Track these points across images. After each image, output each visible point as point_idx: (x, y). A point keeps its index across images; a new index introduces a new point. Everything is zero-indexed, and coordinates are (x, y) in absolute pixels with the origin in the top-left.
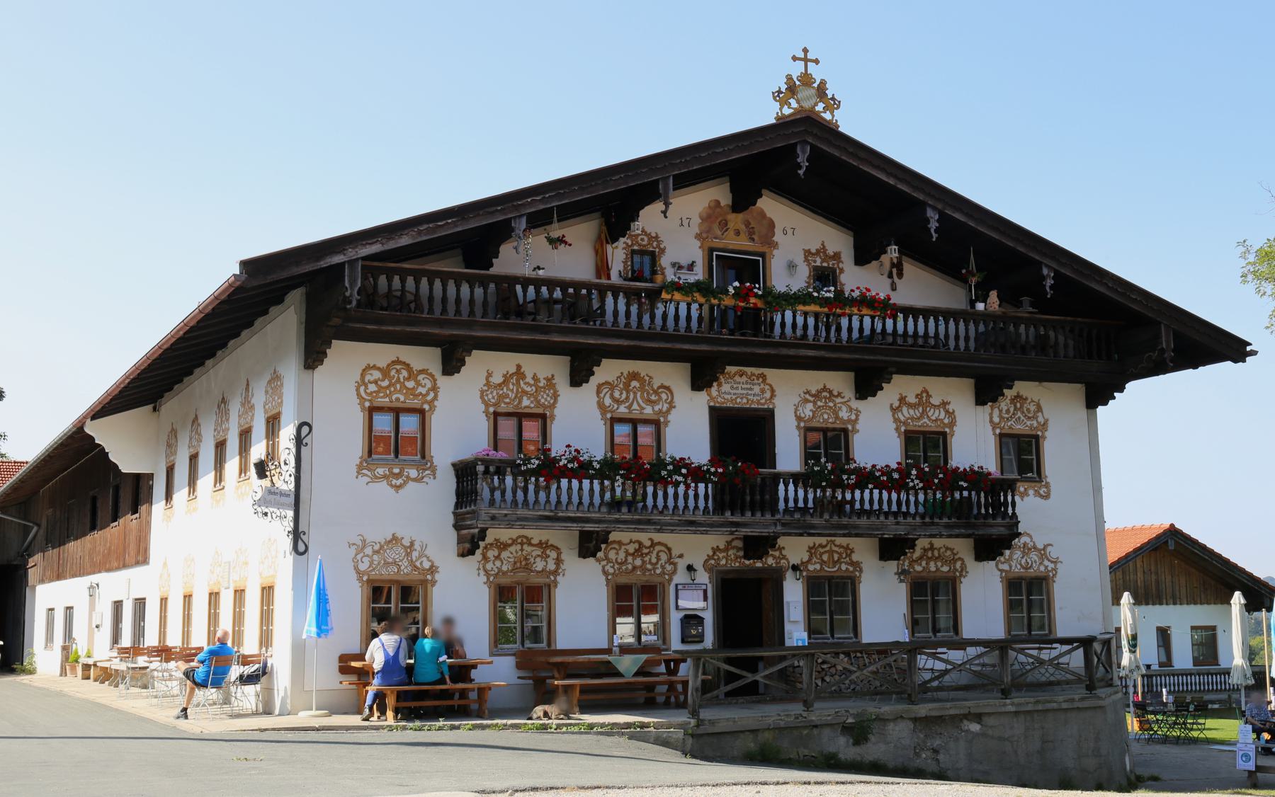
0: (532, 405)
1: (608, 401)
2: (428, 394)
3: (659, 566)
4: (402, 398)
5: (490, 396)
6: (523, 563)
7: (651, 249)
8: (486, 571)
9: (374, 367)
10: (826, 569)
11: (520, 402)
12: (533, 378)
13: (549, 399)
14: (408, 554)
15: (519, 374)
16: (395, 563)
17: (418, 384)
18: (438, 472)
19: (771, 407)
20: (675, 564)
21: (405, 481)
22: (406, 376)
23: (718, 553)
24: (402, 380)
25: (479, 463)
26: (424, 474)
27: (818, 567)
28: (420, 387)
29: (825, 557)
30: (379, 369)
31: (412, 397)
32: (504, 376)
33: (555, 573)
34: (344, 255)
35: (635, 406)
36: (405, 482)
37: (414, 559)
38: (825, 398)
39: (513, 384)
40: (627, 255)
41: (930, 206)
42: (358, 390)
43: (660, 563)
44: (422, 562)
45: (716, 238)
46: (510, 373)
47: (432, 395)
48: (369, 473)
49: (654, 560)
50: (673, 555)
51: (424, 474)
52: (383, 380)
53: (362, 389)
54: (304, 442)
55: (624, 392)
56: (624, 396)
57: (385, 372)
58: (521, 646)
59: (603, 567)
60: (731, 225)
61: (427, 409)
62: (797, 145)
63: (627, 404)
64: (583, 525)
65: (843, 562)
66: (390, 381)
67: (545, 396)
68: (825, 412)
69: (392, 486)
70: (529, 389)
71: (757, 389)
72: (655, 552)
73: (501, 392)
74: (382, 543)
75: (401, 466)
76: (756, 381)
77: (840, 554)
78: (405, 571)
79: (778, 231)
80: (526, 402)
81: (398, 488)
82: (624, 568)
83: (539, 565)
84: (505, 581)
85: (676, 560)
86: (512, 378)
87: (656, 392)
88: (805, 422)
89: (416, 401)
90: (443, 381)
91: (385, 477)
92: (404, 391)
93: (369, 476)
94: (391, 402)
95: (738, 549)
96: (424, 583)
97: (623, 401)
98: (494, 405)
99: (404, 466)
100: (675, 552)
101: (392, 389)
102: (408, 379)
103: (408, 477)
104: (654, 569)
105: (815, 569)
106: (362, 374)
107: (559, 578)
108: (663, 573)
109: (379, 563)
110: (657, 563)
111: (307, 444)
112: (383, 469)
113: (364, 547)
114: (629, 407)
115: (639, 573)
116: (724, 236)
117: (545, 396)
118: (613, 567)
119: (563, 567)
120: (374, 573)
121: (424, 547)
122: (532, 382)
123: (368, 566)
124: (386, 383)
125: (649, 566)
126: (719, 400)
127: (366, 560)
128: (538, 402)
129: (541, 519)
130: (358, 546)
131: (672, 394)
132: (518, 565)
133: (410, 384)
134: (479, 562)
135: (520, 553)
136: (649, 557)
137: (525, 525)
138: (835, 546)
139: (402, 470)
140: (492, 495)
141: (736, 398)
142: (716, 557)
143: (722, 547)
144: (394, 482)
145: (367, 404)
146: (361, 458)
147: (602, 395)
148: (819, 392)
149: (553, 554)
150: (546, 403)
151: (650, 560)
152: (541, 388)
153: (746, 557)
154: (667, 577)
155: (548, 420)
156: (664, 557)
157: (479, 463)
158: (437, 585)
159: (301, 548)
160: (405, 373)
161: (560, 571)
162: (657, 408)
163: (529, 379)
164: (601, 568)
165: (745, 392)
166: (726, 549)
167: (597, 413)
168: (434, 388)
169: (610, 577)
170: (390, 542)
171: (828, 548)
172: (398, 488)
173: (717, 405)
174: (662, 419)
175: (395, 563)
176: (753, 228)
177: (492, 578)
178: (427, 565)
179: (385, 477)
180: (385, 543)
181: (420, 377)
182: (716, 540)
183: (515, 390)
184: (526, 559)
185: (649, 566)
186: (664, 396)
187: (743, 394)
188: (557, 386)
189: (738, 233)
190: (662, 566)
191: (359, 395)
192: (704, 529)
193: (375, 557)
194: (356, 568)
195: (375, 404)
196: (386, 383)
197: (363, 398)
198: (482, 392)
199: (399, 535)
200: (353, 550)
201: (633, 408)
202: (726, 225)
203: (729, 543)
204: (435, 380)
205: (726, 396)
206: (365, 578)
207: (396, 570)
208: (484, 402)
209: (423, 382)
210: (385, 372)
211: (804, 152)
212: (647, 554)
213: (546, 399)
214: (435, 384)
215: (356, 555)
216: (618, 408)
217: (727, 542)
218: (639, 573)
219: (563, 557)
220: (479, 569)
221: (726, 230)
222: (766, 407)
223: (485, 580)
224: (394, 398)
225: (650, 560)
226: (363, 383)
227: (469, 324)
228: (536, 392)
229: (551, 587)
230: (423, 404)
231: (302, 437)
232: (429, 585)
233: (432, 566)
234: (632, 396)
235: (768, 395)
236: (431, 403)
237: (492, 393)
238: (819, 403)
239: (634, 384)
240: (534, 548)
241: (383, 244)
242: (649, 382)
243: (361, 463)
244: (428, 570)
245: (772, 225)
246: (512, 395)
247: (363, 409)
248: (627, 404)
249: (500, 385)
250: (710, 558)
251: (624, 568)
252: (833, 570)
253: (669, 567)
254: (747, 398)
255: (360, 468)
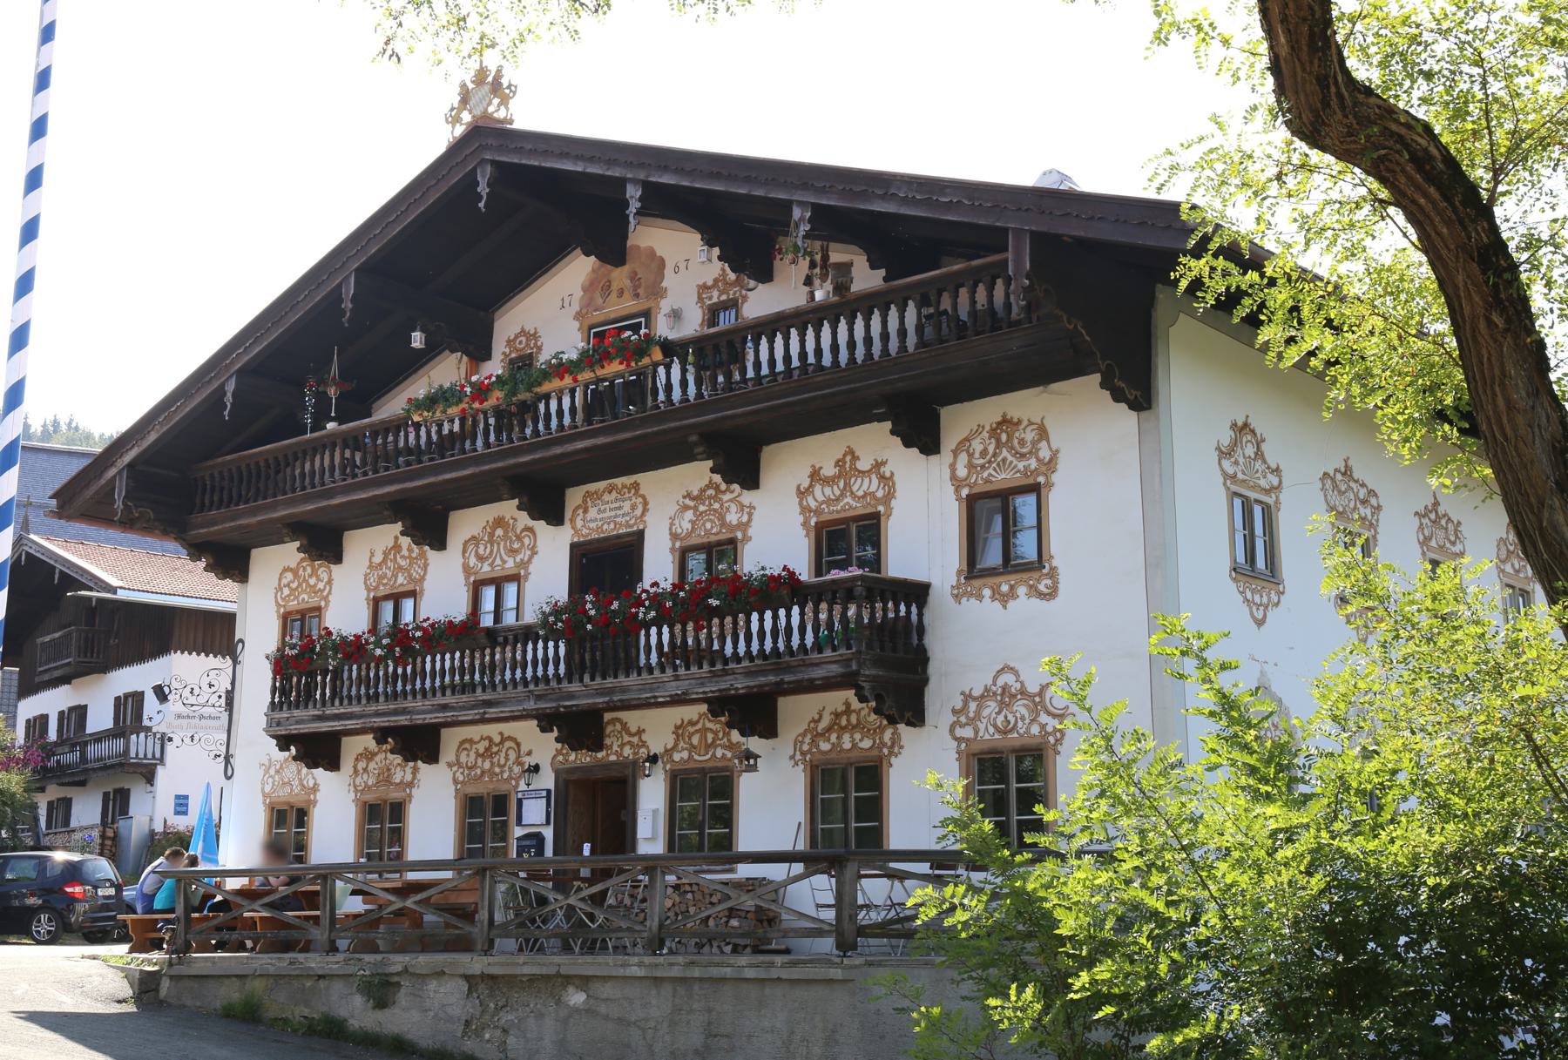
1: (473, 561)
4: (306, 597)
8: (355, 786)
17: (319, 579)
32: (384, 553)
33: (411, 785)
35: (498, 562)
38: (710, 497)
49: (502, 761)
56: (488, 550)
71: (627, 506)
80: (401, 580)
87: (519, 538)
88: (681, 539)
98: (376, 588)
100: (524, 749)
104: (502, 772)
108: (510, 778)
114: (491, 565)
119: (418, 776)
125: (497, 770)
127: (270, 780)
133: (312, 581)
148: (703, 491)
156: (512, 755)
159: (229, 773)
165: (613, 514)
174: (522, 572)
184: (389, 770)
185: (497, 770)
186: (526, 541)
194: (263, 790)
198: (366, 575)
200: (262, 772)
205: (592, 525)
212: (496, 753)
226: (280, 589)
235: (638, 512)
236: (326, 598)
238: (702, 508)
239: (499, 532)
246: (389, 574)
249: (380, 564)
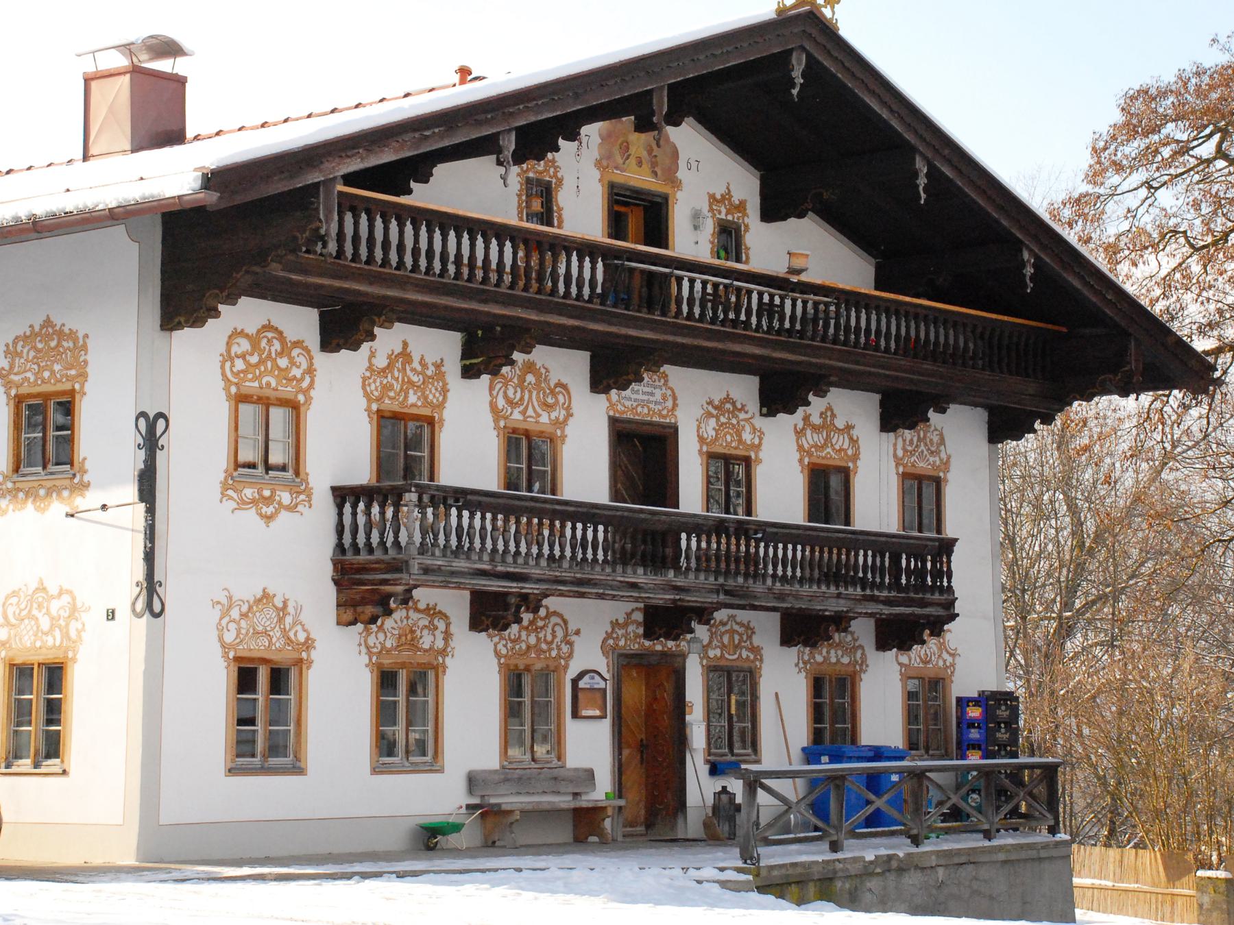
0: (419, 403)
1: (501, 403)
2: (302, 379)
3: (554, 646)
4: (274, 384)
5: (373, 387)
6: (409, 637)
7: (548, 179)
8: (368, 647)
9: (242, 334)
10: (727, 656)
11: (406, 397)
12: (420, 363)
13: (437, 395)
14: (281, 620)
15: (405, 355)
16: (266, 633)
17: (293, 363)
18: (314, 497)
19: (673, 421)
20: (570, 644)
21: (276, 510)
22: (279, 350)
23: (617, 630)
24: (273, 355)
25: (413, 489)
26: (299, 500)
27: (718, 652)
28: (294, 368)
29: (726, 639)
30: (247, 336)
31: (284, 381)
32: (389, 357)
33: (443, 652)
34: (321, 171)
35: (530, 412)
36: (277, 512)
37: (287, 627)
38: (728, 411)
39: (398, 370)
40: (521, 184)
41: (921, 154)
42: (222, 367)
43: (555, 641)
44: (296, 632)
45: (617, 168)
46: (396, 353)
47: (307, 380)
48: (234, 495)
49: (549, 638)
50: (570, 631)
51: (299, 500)
52: (252, 354)
53: (228, 364)
54: (160, 443)
55: (519, 390)
56: (518, 396)
57: (254, 341)
58: (405, 759)
59: (496, 645)
60: (633, 150)
61: (302, 402)
62: (791, 54)
63: (522, 408)
64: (520, 585)
65: (744, 647)
66: (260, 355)
67: (433, 391)
68: (728, 433)
69: (261, 515)
70: (415, 379)
71: (658, 394)
72: (550, 626)
73: (385, 382)
74: (251, 602)
75: (271, 487)
76: (657, 383)
77: (741, 635)
78: (277, 645)
79: (682, 163)
80: (412, 398)
81: (268, 518)
82: (517, 647)
83: (426, 641)
84: (387, 661)
85: (574, 638)
86: (397, 361)
87: (552, 392)
88: (707, 444)
89: (289, 389)
90: (323, 361)
91: (254, 502)
92: (276, 373)
93: (235, 500)
94: (261, 388)
95: (638, 624)
96: (299, 662)
97: (517, 403)
98: (378, 400)
99: (276, 487)
100: (572, 627)
101: (263, 369)
102: (280, 354)
103: (280, 503)
104: (550, 650)
105: (716, 656)
106: (228, 343)
107: (448, 660)
108: (559, 657)
109: (247, 634)
110: (552, 642)
111: (163, 446)
112: (252, 490)
113: (230, 607)
114: (524, 413)
115: (533, 655)
116: (625, 166)
117: (433, 391)
118: (505, 646)
119: (452, 644)
120: (241, 647)
121: (299, 609)
122: (419, 368)
123: (234, 636)
124: (254, 359)
125: (544, 646)
126: (620, 407)
127: (232, 626)
128: (426, 398)
129: (477, 574)
130: (223, 605)
131: (569, 393)
132: (404, 638)
133: (283, 362)
134: (360, 634)
135: (405, 622)
136: (544, 632)
137: (461, 583)
138: (737, 623)
139: (273, 492)
140: (423, 538)
141: (637, 406)
142: (615, 635)
143: (621, 621)
144: (264, 510)
145: (233, 390)
146: (226, 472)
147: (495, 393)
148: (723, 402)
149: (441, 625)
150: (435, 401)
151: (545, 636)
152: (430, 377)
153: (648, 635)
154: (563, 662)
155: (437, 426)
156: (560, 633)
157: (413, 489)
158: (314, 665)
159: (157, 607)
160: (277, 346)
161: (449, 649)
162: (553, 415)
163: (416, 365)
164: (492, 645)
165: (645, 397)
166: (626, 625)
167: (488, 418)
168: (310, 371)
169: (502, 661)
170: (260, 600)
171: (728, 627)
172: (268, 518)
173: (617, 415)
174: (559, 433)
175: (266, 633)
176: (656, 156)
177: (374, 659)
178: (302, 637)
179: (254, 502)
180: (255, 602)
181: (295, 352)
182: (617, 610)
183: (400, 379)
184: (412, 632)
185: (544, 646)
186: (561, 398)
187: (644, 400)
188: (447, 375)
189: (640, 163)
190: (557, 646)
191: (224, 374)
192: (647, 595)
193: (243, 624)
194: (221, 639)
195: (244, 391)
196: (254, 359)
197: (229, 380)
198: (364, 379)
199: (271, 591)
200: (217, 613)
201: (528, 414)
202: (628, 148)
203: (629, 615)
204: (311, 358)
205: (628, 403)
206: (231, 655)
207: (267, 644)
208: (367, 395)
209: (297, 360)
210: (254, 341)
211: (799, 64)
212: (542, 628)
213: (434, 396)
214: (312, 364)
215: (221, 619)
216: (511, 413)
217: (626, 614)
218: (533, 655)
219: (453, 629)
220: (360, 645)
221: (627, 158)
222: (668, 421)
223: (367, 661)
224: (264, 381)
225: (545, 636)
226: (228, 357)
227: (402, 283)
228: (423, 383)
229: (439, 669)
230: (297, 392)
231: (158, 434)
232: (304, 667)
233: (308, 639)
234: (526, 397)
235: (669, 404)
236: (306, 392)
237: (375, 381)
238: (723, 420)
239: (530, 378)
240: (421, 616)
241: (362, 159)
242: (546, 377)
243: (226, 479)
244: (303, 644)
245: (675, 154)
246: (397, 387)
247: (229, 396)
248: (522, 408)
249: (384, 370)
250: (609, 636)
251: (517, 647)
252: (731, 657)
253: (565, 648)
254: (648, 407)
255: (225, 487)
